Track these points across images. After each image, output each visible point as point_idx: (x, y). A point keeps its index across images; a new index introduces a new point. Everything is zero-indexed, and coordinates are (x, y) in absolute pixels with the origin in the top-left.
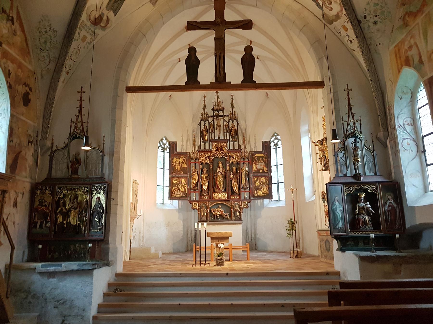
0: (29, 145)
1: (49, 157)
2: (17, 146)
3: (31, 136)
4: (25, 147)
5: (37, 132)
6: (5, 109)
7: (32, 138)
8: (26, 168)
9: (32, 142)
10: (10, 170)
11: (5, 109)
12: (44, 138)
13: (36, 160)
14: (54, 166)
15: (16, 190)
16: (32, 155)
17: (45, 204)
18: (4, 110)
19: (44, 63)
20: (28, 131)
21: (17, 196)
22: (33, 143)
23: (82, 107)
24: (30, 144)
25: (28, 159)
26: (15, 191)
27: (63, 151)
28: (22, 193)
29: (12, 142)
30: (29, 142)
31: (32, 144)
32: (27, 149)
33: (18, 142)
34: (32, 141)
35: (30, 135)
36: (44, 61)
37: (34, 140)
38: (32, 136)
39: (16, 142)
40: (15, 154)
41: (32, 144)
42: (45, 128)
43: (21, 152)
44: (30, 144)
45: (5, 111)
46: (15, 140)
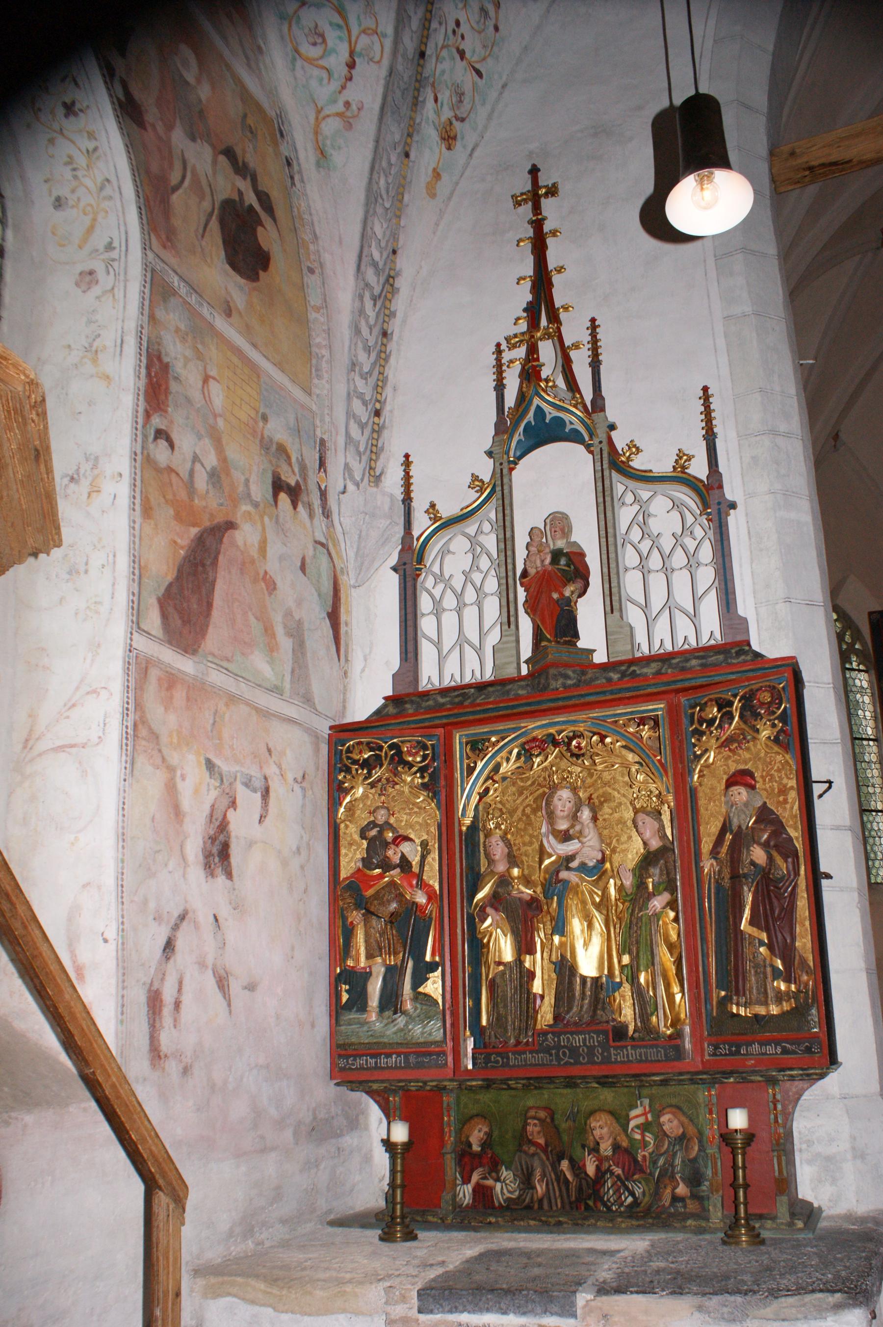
0: (280, 503)
1: (395, 578)
2: (201, 482)
3: (289, 458)
4: (256, 505)
5: (323, 442)
6: (111, 243)
7: (296, 470)
8: (268, 630)
9: (295, 493)
10: (164, 616)
11: (111, 243)
12: (358, 478)
13: (330, 602)
14: (427, 625)
15: (217, 761)
16: (303, 568)
17: (403, 857)
18: (109, 247)
19: (325, 75)
20: (265, 418)
21: (225, 801)
22: (304, 497)
23: (552, 264)
24: (283, 497)
25: (279, 584)
26: (210, 765)
27: (471, 530)
28: (258, 783)
29: (163, 443)
30: (278, 486)
31: (295, 505)
32: (266, 519)
33: (211, 460)
34: (297, 483)
35: (282, 450)
36: (321, 62)
37: (305, 480)
38: (294, 460)
39: (196, 459)
40: (194, 531)
41: (295, 505)
42: (362, 426)
43: (230, 525)
44: (283, 497)
45: (114, 254)
46: (186, 442)
